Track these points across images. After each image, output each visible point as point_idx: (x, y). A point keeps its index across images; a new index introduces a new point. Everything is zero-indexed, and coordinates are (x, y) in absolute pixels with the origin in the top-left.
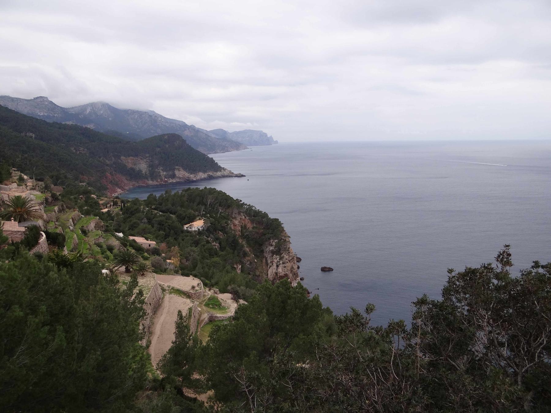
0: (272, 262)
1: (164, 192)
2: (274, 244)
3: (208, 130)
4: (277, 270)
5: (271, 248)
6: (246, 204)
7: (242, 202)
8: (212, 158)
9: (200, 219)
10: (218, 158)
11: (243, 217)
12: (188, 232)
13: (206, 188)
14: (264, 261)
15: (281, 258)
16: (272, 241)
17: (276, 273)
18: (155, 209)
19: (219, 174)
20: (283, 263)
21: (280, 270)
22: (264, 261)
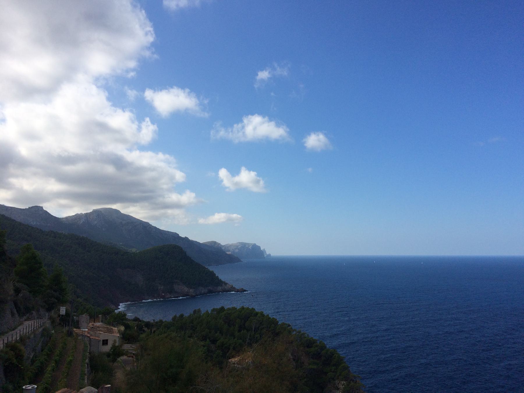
2: (341, 387)
8: (213, 272)
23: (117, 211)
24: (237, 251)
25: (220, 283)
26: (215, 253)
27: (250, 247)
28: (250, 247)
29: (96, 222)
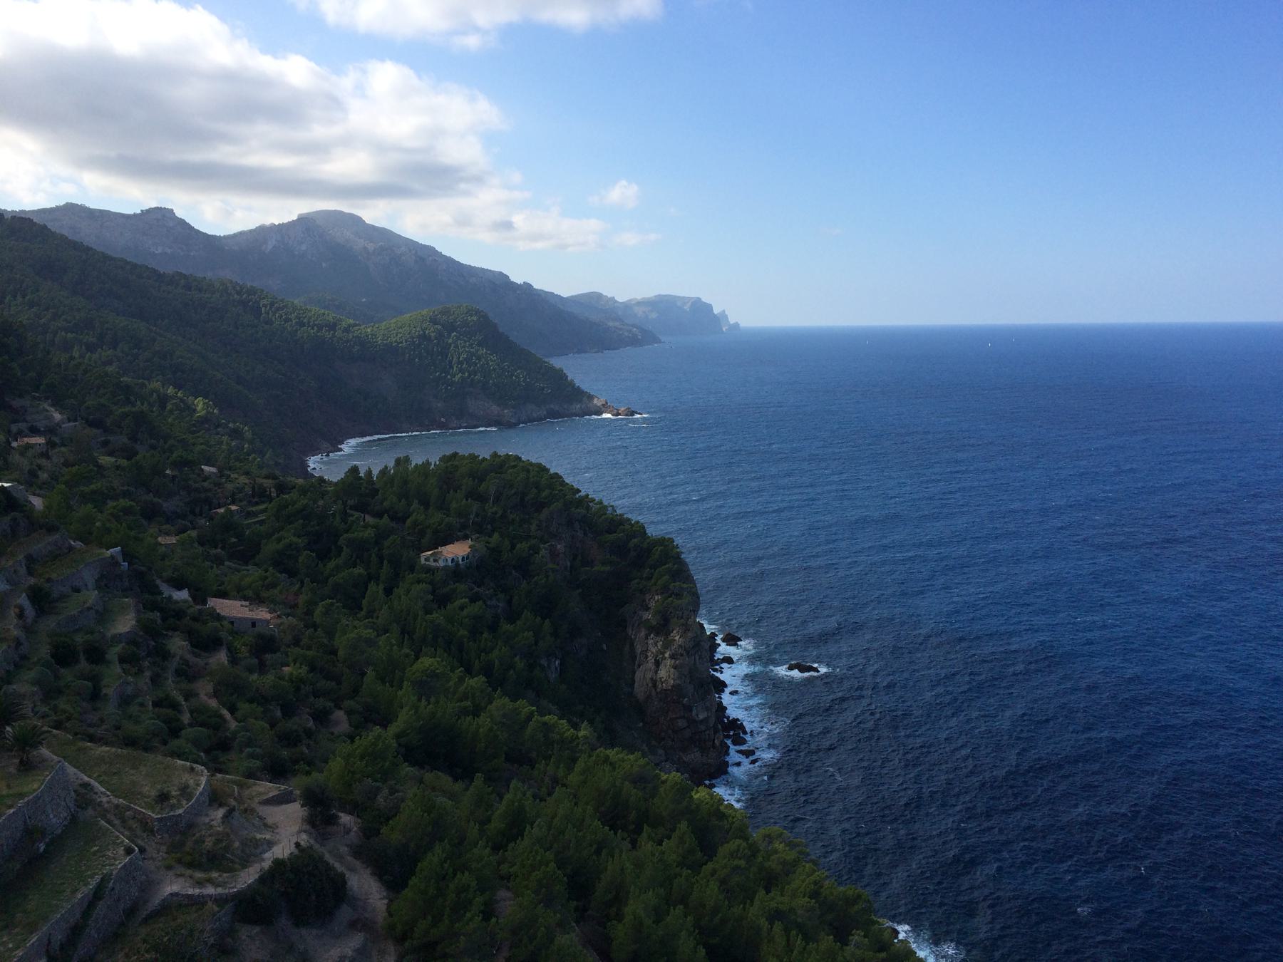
0: (645, 652)
1: (391, 464)
2: (652, 604)
3: (565, 294)
4: (656, 672)
5: (647, 616)
6: (593, 500)
7: (582, 494)
9: (466, 537)
10: (580, 370)
11: (580, 534)
12: (429, 570)
13: (495, 455)
14: (627, 648)
15: (667, 646)
16: (648, 596)
17: (654, 682)
18: (355, 508)
19: (577, 407)
20: (672, 657)
21: (663, 673)
22: (627, 648)
23: (357, 220)
24: (654, 315)
25: (577, 395)
26: (590, 325)
27: (687, 308)
28: (687, 308)
29: (304, 248)
